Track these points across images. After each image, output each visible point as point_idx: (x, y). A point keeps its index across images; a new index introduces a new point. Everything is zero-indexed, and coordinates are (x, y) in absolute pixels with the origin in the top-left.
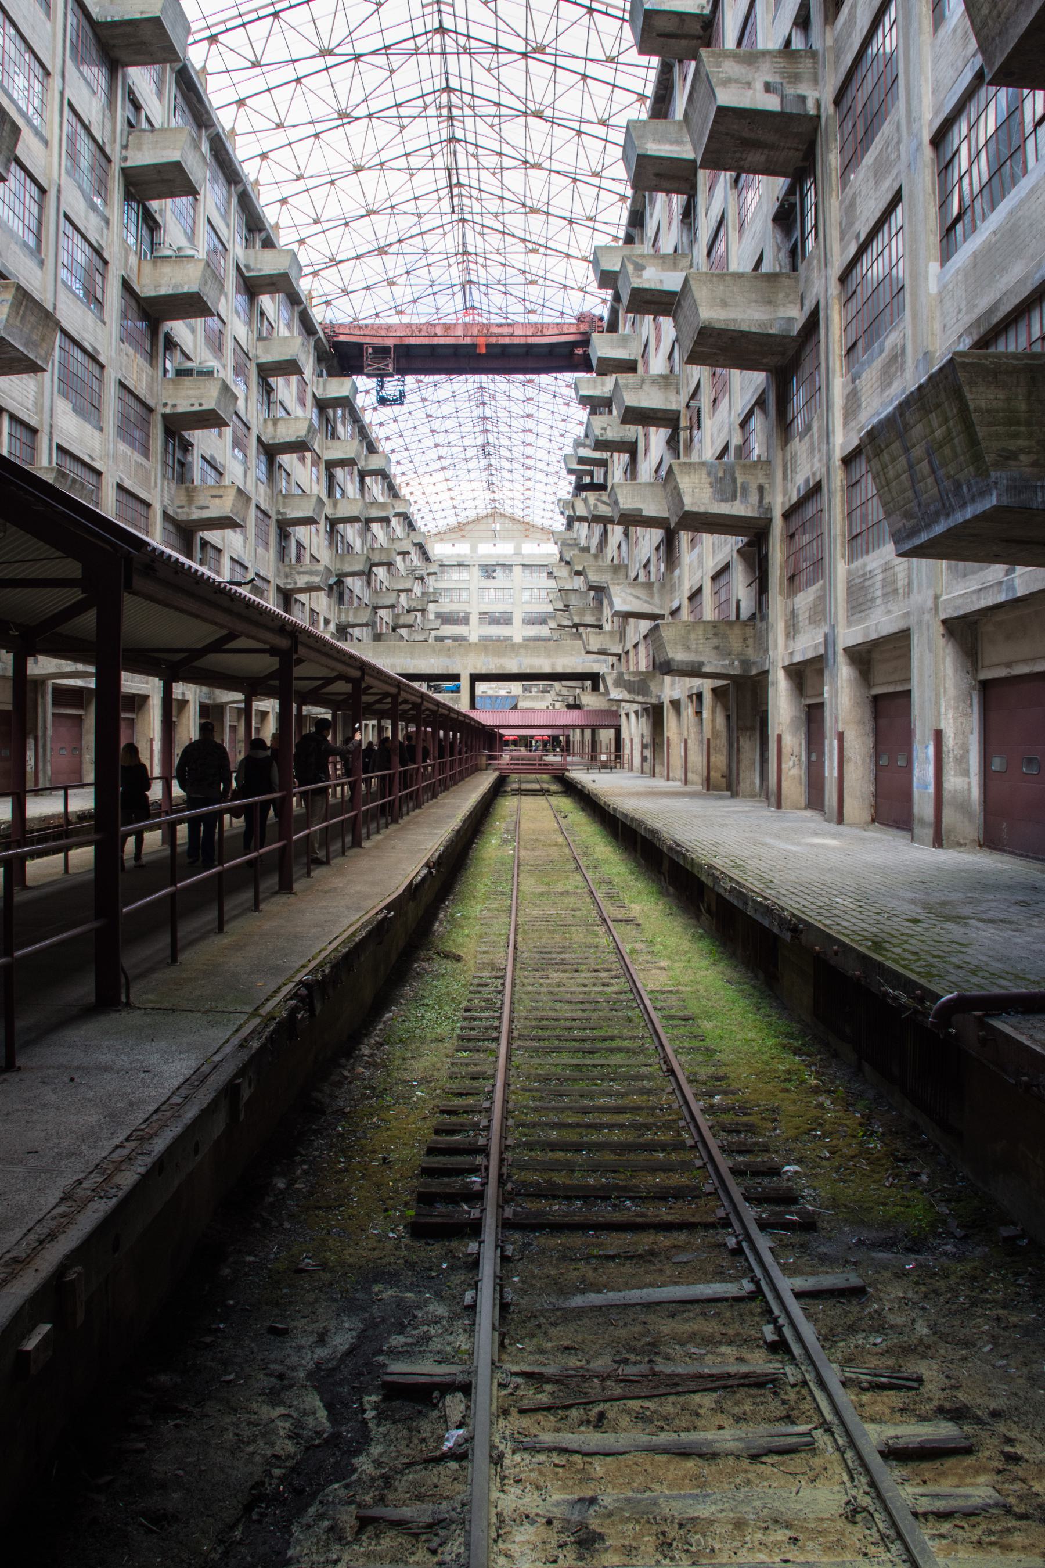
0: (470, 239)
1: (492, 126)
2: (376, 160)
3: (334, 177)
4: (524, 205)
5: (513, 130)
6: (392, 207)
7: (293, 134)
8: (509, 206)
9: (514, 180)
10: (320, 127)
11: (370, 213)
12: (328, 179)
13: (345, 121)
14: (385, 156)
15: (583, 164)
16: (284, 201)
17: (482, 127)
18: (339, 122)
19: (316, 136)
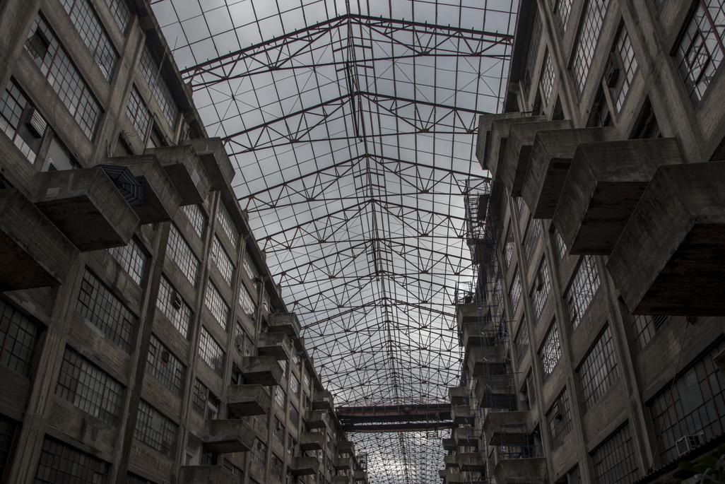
0: (399, 392)
1: (406, 334)
2: (359, 349)
3: (343, 356)
4: (420, 380)
5: (415, 336)
6: (366, 367)
7: (327, 339)
8: (413, 365)
9: (415, 355)
10: (338, 336)
11: (357, 370)
12: (340, 357)
13: (348, 333)
14: (363, 347)
15: (441, 364)
16: (323, 366)
17: (402, 336)
18: (344, 334)
19: (336, 340)
